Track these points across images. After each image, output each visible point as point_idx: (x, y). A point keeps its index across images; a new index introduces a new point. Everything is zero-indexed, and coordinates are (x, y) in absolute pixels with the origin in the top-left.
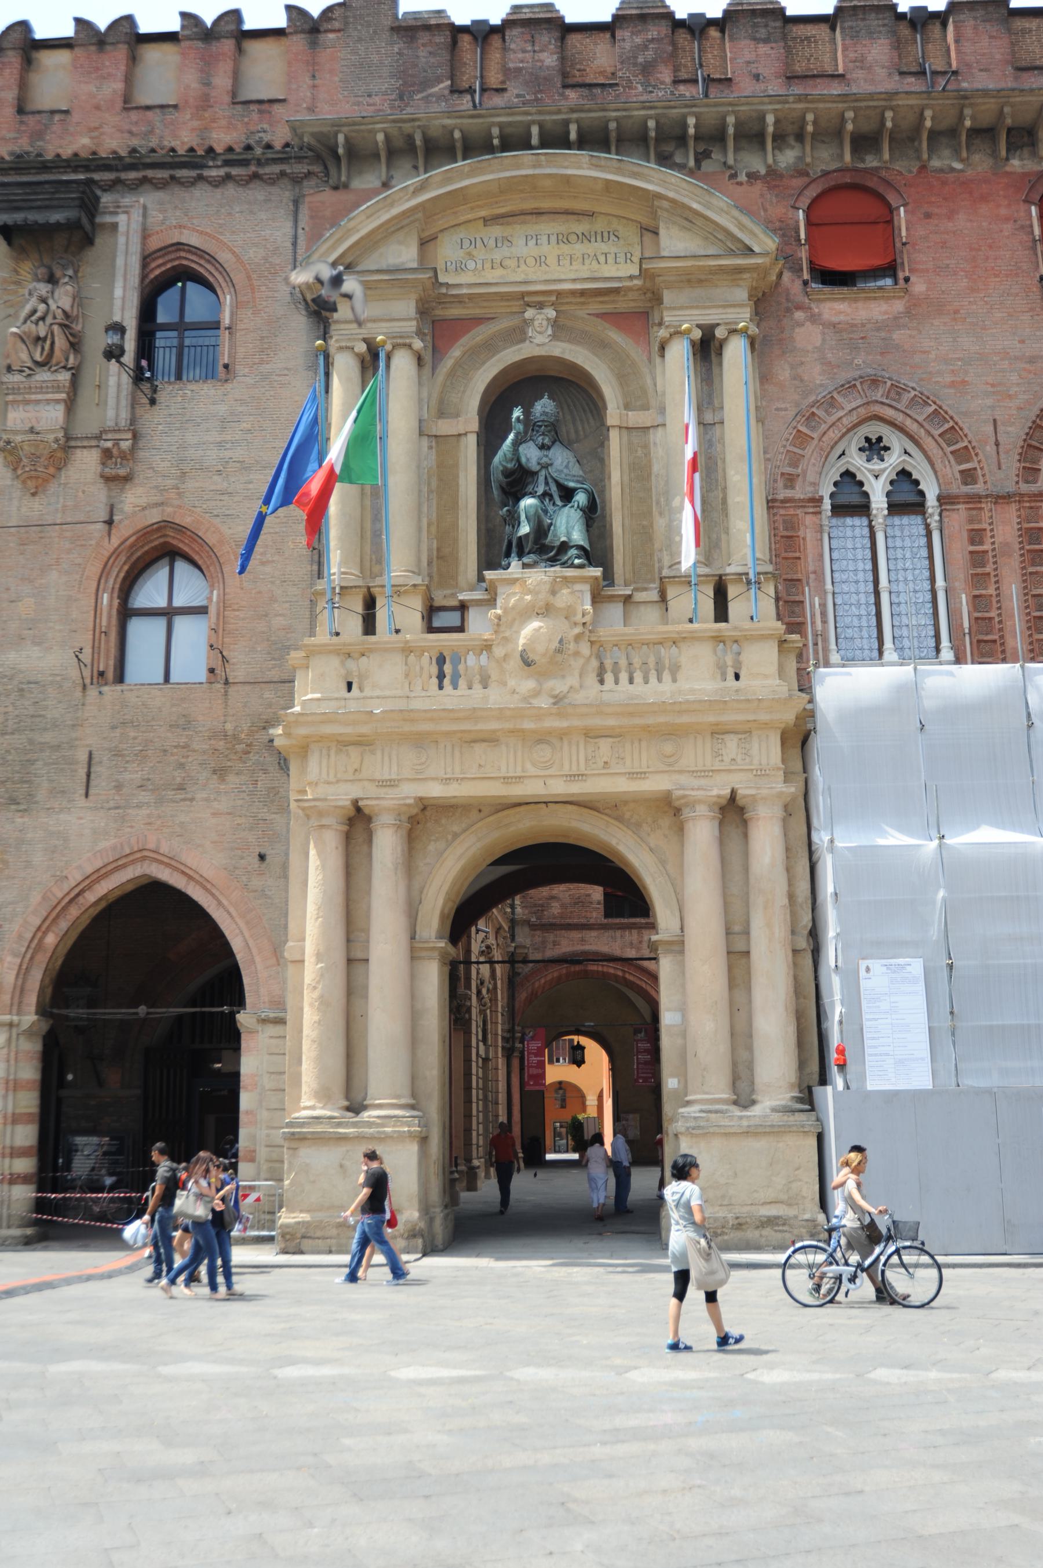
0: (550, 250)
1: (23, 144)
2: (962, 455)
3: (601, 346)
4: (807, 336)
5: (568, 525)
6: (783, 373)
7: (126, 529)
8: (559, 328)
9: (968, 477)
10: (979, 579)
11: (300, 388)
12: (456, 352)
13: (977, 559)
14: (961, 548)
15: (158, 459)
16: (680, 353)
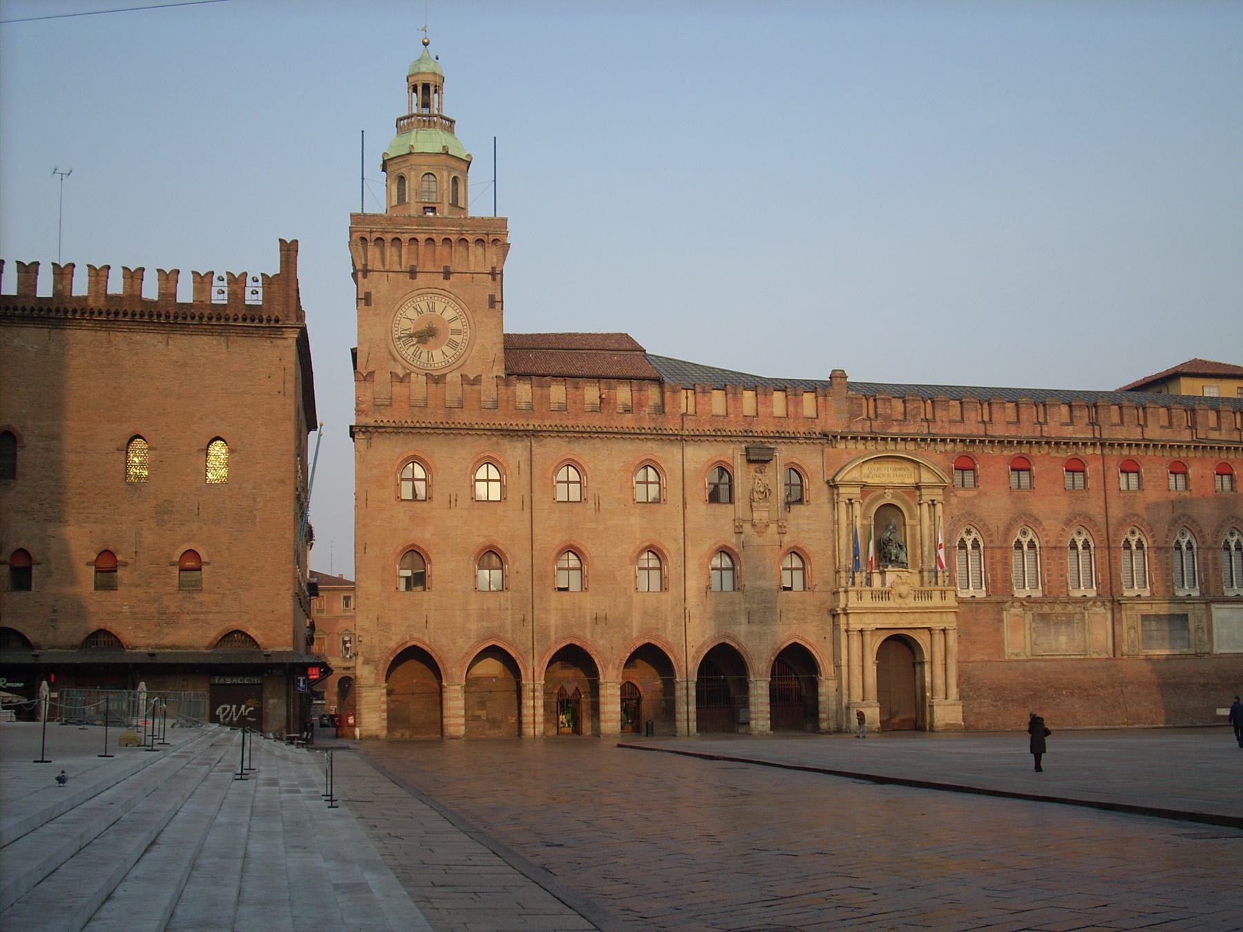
0: (891, 472)
1: (746, 428)
2: (990, 536)
3: (903, 501)
4: (954, 500)
5: (902, 557)
6: (948, 510)
7: (784, 548)
8: (894, 496)
9: (991, 542)
10: (993, 569)
11: (827, 508)
12: (867, 500)
13: (992, 564)
14: (988, 561)
15: (791, 528)
16: (925, 507)
